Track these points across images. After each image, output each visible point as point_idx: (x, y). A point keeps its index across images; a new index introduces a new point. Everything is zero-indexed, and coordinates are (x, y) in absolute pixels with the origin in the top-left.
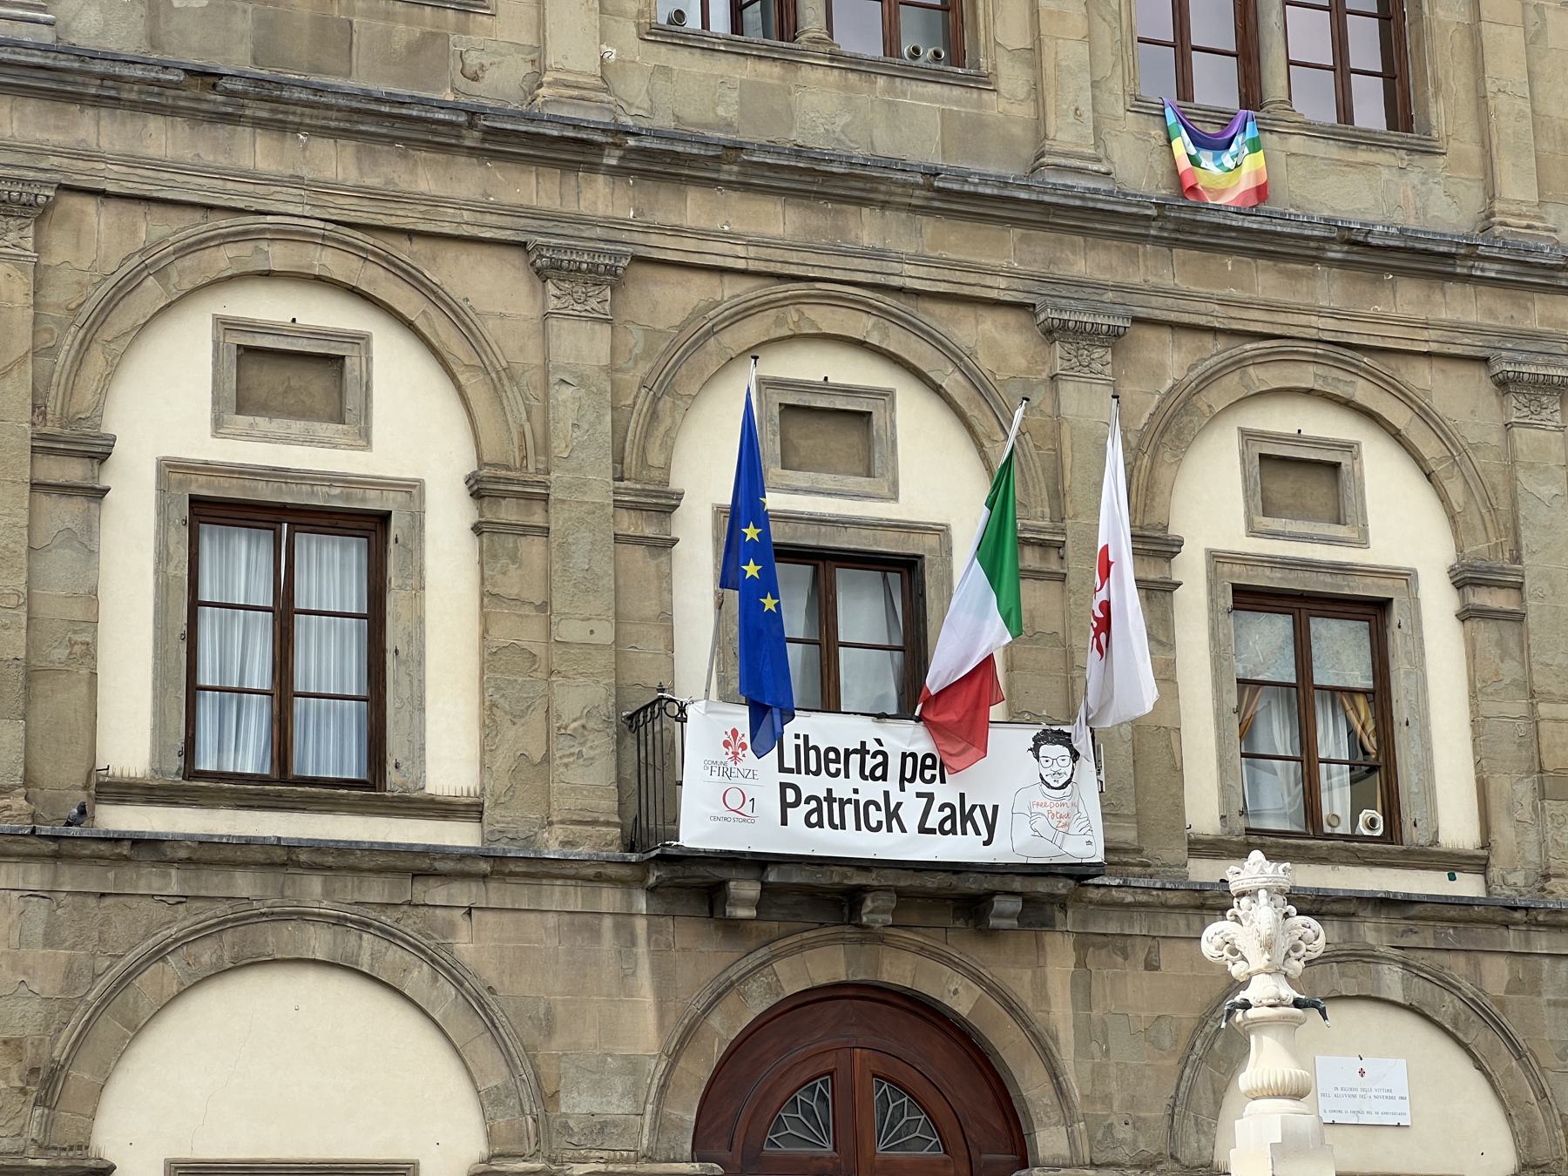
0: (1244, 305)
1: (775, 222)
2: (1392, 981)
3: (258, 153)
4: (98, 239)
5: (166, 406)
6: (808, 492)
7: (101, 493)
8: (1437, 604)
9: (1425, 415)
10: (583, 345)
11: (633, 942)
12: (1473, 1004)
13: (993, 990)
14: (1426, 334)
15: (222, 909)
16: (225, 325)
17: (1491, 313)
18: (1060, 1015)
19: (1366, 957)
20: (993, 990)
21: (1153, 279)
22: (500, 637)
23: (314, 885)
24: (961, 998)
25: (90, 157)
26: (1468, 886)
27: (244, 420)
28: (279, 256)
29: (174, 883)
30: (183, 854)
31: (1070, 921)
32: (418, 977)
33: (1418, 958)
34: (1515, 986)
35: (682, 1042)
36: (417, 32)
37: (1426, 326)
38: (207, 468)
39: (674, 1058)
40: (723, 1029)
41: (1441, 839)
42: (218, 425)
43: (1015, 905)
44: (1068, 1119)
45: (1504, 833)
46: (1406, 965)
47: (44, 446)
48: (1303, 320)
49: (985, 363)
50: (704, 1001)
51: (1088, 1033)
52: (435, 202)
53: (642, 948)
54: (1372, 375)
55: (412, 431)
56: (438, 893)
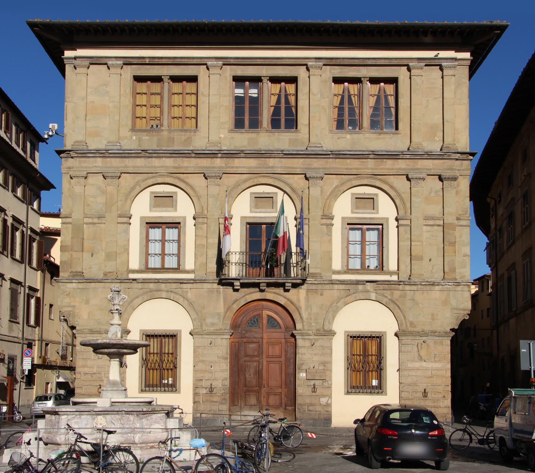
0: (351, 169)
1: (252, 163)
2: (373, 296)
3: (156, 162)
4: (127, 181)
5: (142, 207)
6: (259, 212)
7: (130, 224)
8: (393, 224)
9: (392, 187)
10: (214, 190)
11: (220, 293)
12: (391, 300)
13: (288, 300)
14: (392, 171)
16: (152, 193)
17: (408, 165)
18: (302, 304)
19: (368, 291)
20: (288, 300)
21: (331, 166)
22: (198, 243)
23: (163, 285)
24: (282, 301)
25: (127, 167)
26: (395, 278)
27: (155, 209)
28: (160, 180)
29: (140, 286)
31: (305, 287)
32: (181, 300)
34: (401, 296)
35: (228, 310)
36: (186, 137)
37: (392, 169)
38: (148, 217)
39: (226, 313)
40: (236, 307)
42: (151, 210)
43: (290, 285)
44: (303, 321)
45: (402, 267)
47: (120, 216)
48: (364, 171)
49: (295, 186)
51: (308, 307)
52: (187, 167)
54: (379, 179)
55: (184, 208)
56: (184, 286)
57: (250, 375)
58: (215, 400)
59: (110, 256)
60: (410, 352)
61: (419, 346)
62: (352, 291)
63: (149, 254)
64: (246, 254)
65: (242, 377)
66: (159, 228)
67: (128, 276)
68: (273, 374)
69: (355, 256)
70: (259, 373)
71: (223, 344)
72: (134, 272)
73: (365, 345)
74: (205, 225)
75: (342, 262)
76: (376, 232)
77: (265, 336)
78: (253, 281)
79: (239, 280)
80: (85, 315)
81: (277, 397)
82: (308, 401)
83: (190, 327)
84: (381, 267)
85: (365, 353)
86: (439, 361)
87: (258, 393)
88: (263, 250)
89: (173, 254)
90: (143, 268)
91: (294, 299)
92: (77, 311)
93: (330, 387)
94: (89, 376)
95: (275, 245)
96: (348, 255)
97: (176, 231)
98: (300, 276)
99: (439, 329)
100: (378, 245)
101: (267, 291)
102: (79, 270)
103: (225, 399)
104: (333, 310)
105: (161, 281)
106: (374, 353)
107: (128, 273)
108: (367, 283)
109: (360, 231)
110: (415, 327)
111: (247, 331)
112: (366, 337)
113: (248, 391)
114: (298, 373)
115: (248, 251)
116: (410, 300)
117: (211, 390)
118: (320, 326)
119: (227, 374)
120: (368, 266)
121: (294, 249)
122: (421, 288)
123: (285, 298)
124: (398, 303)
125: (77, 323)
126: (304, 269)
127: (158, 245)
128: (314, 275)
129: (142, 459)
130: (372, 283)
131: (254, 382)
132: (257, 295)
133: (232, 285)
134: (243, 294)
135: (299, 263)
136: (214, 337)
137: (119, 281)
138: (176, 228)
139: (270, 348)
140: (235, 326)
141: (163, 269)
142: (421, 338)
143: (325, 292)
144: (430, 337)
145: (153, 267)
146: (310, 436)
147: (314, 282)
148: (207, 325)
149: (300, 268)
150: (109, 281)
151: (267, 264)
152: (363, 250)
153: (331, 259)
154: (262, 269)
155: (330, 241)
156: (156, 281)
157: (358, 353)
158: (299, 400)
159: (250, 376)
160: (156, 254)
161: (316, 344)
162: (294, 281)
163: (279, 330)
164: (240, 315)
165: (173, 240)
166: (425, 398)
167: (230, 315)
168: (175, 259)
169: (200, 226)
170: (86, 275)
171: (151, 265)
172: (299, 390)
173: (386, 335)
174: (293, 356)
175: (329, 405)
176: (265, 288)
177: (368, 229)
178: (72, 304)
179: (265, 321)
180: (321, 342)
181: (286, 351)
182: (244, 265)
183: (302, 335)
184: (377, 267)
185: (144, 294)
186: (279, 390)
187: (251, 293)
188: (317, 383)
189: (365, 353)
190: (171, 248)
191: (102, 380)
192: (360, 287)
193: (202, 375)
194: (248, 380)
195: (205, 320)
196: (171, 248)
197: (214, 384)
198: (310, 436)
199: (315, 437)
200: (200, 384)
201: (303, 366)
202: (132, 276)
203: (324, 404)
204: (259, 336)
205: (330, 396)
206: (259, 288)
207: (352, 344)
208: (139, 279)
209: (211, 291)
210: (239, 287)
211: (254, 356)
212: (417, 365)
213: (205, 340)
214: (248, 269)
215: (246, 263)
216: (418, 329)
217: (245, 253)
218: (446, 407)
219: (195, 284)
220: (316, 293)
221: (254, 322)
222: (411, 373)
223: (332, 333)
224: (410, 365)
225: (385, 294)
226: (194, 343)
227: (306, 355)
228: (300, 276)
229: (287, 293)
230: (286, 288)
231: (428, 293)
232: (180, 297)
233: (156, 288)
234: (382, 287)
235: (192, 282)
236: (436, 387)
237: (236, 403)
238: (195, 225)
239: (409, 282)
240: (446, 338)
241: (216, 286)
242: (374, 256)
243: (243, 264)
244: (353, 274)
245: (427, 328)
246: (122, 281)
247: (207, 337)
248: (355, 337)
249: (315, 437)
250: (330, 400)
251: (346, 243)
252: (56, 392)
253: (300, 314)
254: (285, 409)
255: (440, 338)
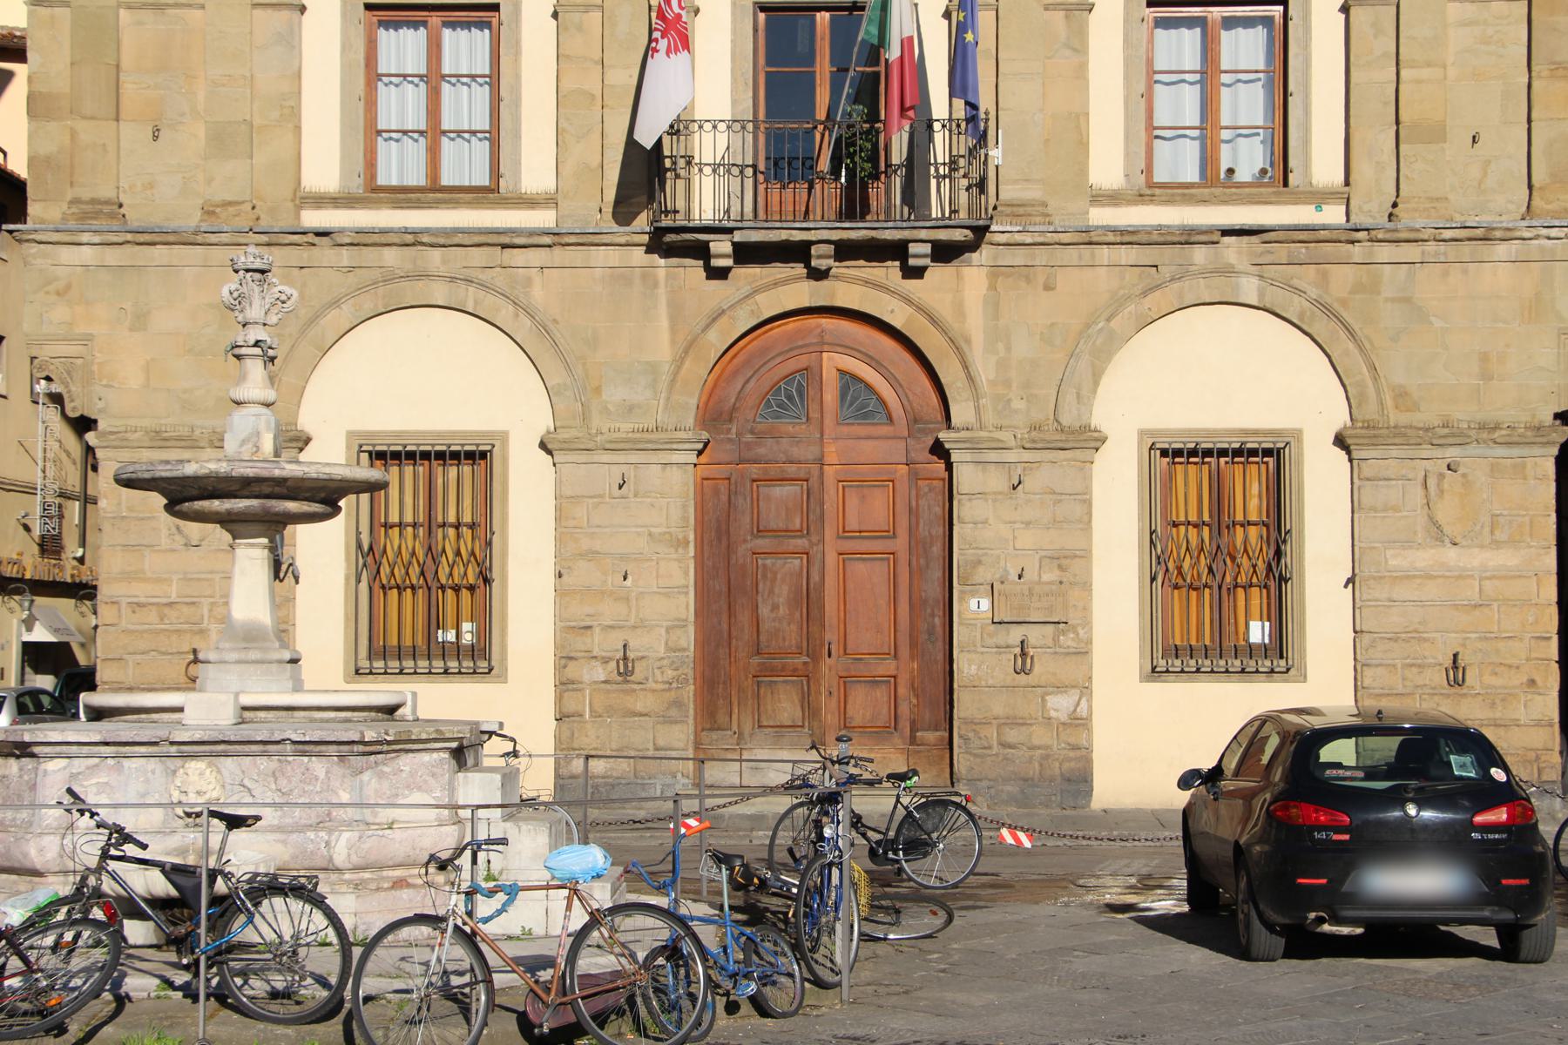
2: (1249, 288)
11: (656, 285)
13: (920, 309)
15: (376, 274)
18: (975, 324)
19: (1228, 271)
20: (920, 309)
23: (436, 254)
24: (897, 316)
26: (1333, 215)
29: (346, 256)
30: (348, 240)
32: (505, 314)
33: (1271, 271)
34: (1358, 288)
35: (686, 352)
39: (679, 362)
40: (718, 339)
41: (1314, 182)
43: (927, 248)
45: (1361, 169)
46: (1261, 277)
50: (703, 324)
53: (662, 291)
56: (518, 257)
57: (775, 607)
58: (639, 707)
59: (226, 140)
60: (1396, 509)
61: (1432, 482)
62: (1166, 271)
63: (379, 132)
64: (756, 128)
65: (744, 618)
66: (415, 25)
67: (298, 217)
68: (865, 605)
69: (1179, 132)
70: (809, 602)
71: (668, 492)
72: (321, 201)
73: (1218, 487)
74: (596, 16)
75: (1127, 155)
76: (1260, 33)
77: (832, 453)
78: (784, 235)
79: (730, 231)
80: (132, 376)
81: (881, 694)
82: (998, 709)
83: (543, 421)
84: (1280, 172)
85: (1220, 519)
86: (1513, 542)
87: (808, 676)
88: (821, 114)
89: (474, 133)
90: (357, 186)
91: (944, 311)
92: (99, 357)
93: (1083, 653)
94: (152, 616)
95: (868, 92)
96: (1150, 127)
97: (482, 38)
98: (963, 214)
99: (1508, 415)
100: (1269, 86)
101: (836, 277)
102: (106, 192)
103: (678, 703)
104: (1092, 346)
105: (425, 239)
106: (1253, 517)
107: (299, 208)
108: (1226, 239)
109: (1198, 30)
110: (1415, 407)
111: (760, 436)
112: (1223, 453)
113: (768, 672)
114: (961, 599)
115: (762, 116)
116: (1393, 300)
117: (626, 666)
118: (1042, 414)
119: (685, 606)
120: (1231, 171)
121: (940, 103)
122: (1437, 254)
123: (908, 301)
124: (1345, 315)
125: (100, 405)
126: (981, 185)
127: (415, 96)
128: (1019, 210)
129: (361, 928)
130: (1245, 239)
131: (791, 634)
132: (802, 293)
133: (701, 252)
134: (746, 290)
135: (962, 162)
136: (634, 457)
137: (264, 238)
138: (481, 25)
139: (853, 502)
140: (714, 415)
141: (434, 192)
142: (1438, 453)
143: (1064, 279)
144: (1472, 450)
145: (394, 182)
146: (1010, 840)
147: (1018, 238)
148: (605, 411)
149: (965, 182)
150: (224, 238)
151: (835, 172)
152: (1208, 106)
153: (1083, 145)
154: (818, 187)
155: (1081, 73)
156: (409, 238)
157: (1193, 518)
158: (965, 706)
159: (776, 611)
160: (405, 132)
161: (1028, 483)
162: (943, 235)
163: (885, 430)
164: (736, 373)
165: (473, 77)
166: (1457, 690)
167: (697, 370)
168: (481, 149)
169: (576, 17)
170: (136, 216)
171: (388, 175)
172: (966, 666)
173: (1299, 440)
174: (939, 530)
175: (1080, 722)
176: (831, 262)
177: (1229, 23)
178: (81, 329)
179: (830, 396)
180: (1048, 474)
181: (913, 512)
182: (749, 172)
183: (974, 446)
184: (1263, 172)
185: (361, 289)
186: (889, 667)
187: (776, 284)
188: (1035, 635)
189: (1220, 519)
190: (465, 107)
191: (202, 632)
192: (1200, 255)
193: (588, 610)
194: (764, 627)
195: (598, 390)
196: (465, 107)
197: (638, 644)
198: (1010, 840)
199: (1027, 844)
200: (580, 643)
201: (981, 569)
202: (313, 219)
203: (1064, 718)
204: (811, 452)
205: (1085, 689)
206: (807, 265)
207: (1169, 480)
208: (341, 231)
209: (620, 276)
210: (729, 262)
211: (788, 532)
212: (1423, 558)
213: (603, 473)
214: (761, 188)
215: (754, 167)
216: (1428, 415)
217: (750, 127)
218: (1538, 724)
219: (557, 250)
220: (1028, 280)
221: (790, 398)
222: (1401, 592)
223: (1092, 440)
224: (1397, 560)
225: (1295, 282)
226: (558, 483)
227: (992, 528)
228: (963, 214)
229: (912, 284)
230: (912, 262)
231: (1465, 272)
232: (501, 301)
233: (409, 266)
234: (1281, 252)
235: (547, 240)
236: (1501, 645)
237: (722, 718)
238: (555, 15)
239: (1391, 230)
240: (1537, 451)
241: (639, 256)
242: (1249, 131)
243: (742, 168)
244: (1170, 202)
245: (1463, 414)
246: (274, 238)
247: (607, 457)
248: (1178, 453)
249: (1027, 844)
250: (1084, 702)
251: (1146, 79)
252: (22, 682)
253: (966, 367)
254: (913, 740)
255: (1516, 451)
